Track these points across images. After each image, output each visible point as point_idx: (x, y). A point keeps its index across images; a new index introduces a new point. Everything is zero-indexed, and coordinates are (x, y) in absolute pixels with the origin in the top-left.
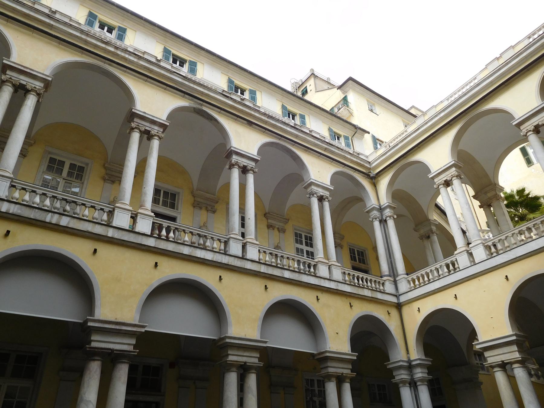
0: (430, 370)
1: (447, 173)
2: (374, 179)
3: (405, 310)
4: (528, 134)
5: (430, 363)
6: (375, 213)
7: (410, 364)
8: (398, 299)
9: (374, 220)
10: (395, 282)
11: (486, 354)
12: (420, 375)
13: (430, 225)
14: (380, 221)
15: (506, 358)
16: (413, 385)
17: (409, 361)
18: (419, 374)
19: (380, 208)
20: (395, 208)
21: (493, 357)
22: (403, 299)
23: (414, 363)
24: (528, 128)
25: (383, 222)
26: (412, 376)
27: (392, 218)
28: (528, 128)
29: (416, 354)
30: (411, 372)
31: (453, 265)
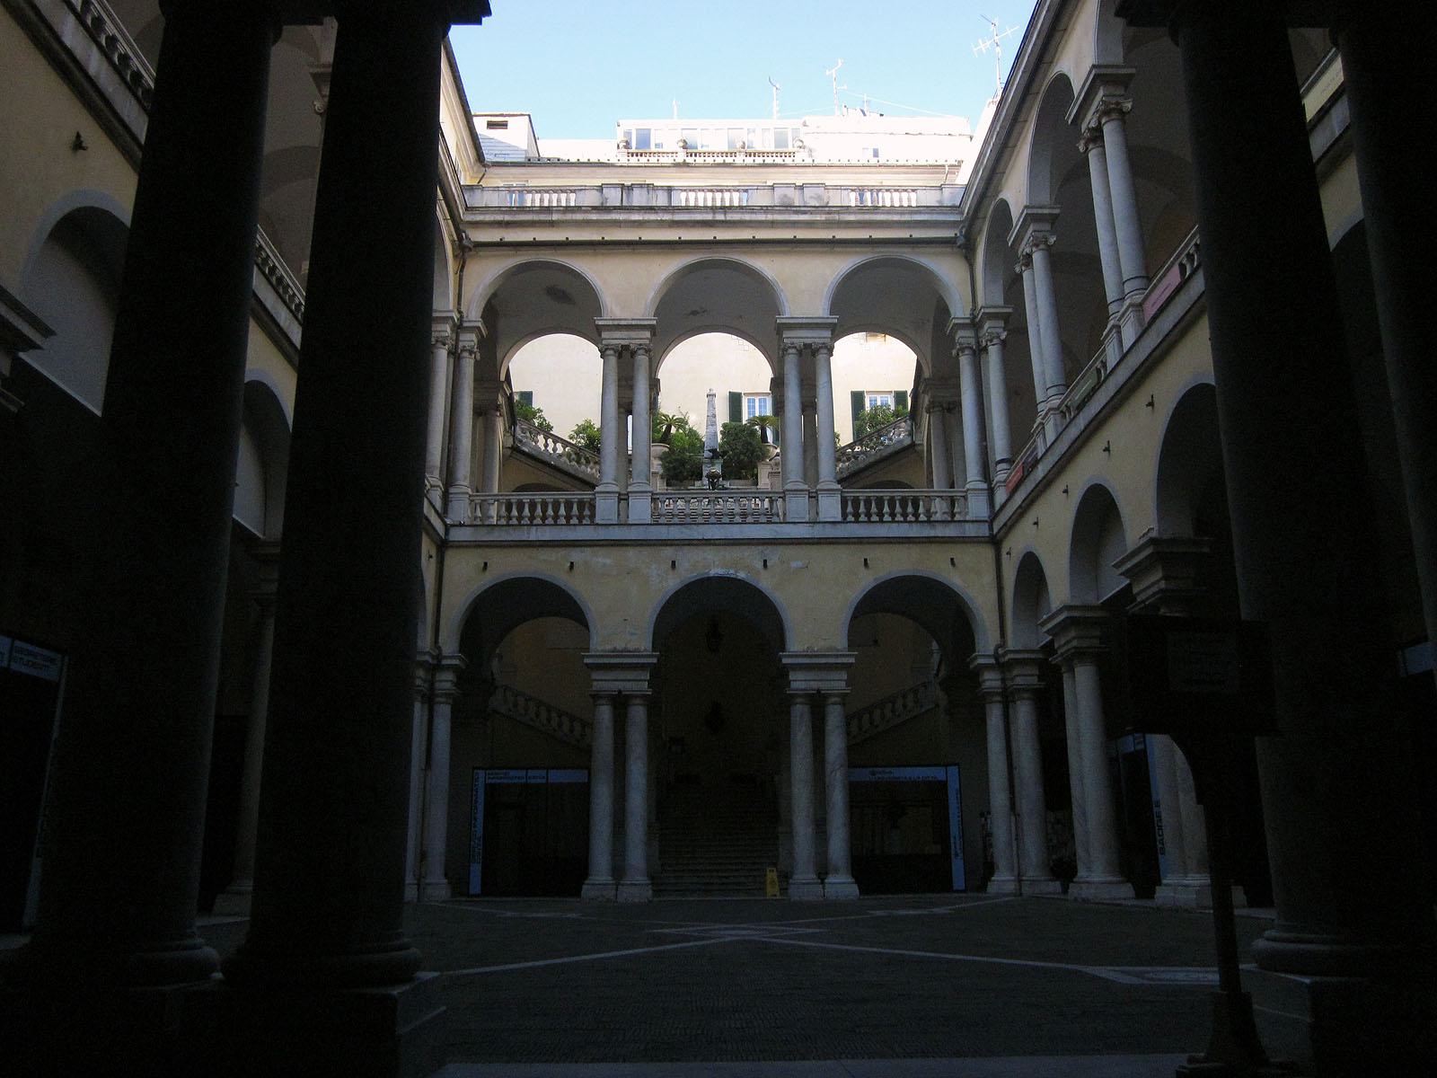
0: (462, 677)
1: (633, 334)
2: (465, 250)
3: (452, 558)
4: (790, 351)
5: (464, 668)
6: (447, 329)
7: (440, 661)
8: (447, 533)
9: (439, 345)
10: (446, 497)
11: (595, 676)
12: (448, 685)
13: (497, 392)
14: (450, 353)
15: (628, 687)
16: (430, 700)
17: (439, 657)
18: (446, 681)
19: (461, 324)
20: (482, 336)
21: (606, 683)
22: (457, 535)
23: (445, 662)
24: (795, 340)
25: (455, 355)
26: (432, 684)
27: (473, 356)
28: (795, 340)
29: (449, 644)
30: (433, 676)
31: (581, 508)
